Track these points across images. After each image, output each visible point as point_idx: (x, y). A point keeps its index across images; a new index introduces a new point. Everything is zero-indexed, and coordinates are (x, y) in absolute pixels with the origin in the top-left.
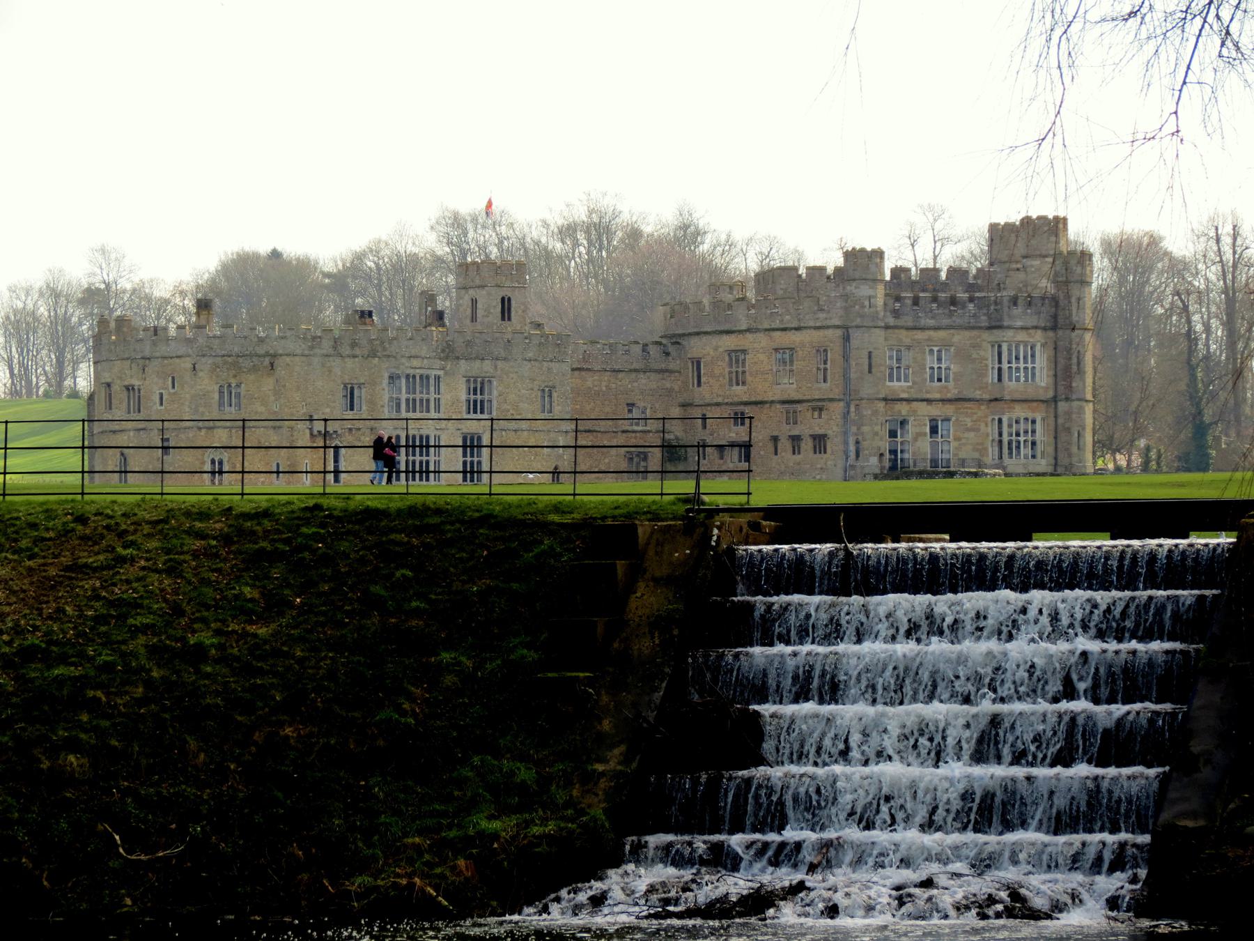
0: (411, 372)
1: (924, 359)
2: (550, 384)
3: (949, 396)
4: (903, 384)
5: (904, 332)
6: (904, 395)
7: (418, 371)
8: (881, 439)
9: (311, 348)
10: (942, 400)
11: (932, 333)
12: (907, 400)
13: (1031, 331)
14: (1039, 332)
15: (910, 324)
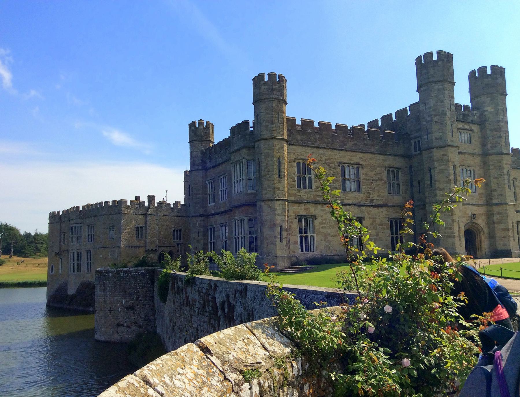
0: (71, 226)
1: (218, 186)
2: (112, 225)
3: (226, 209)
4: (214, 204)
5: (212, 170)
6: (213, 212)
7: (73, 225)
8: (198, 242)
9: (54, 220)
10: (224, 212)
11: (221, 168)
12: (214, 214)
13: (241, 152)
14: (244, 151)
15: (214, 164)
